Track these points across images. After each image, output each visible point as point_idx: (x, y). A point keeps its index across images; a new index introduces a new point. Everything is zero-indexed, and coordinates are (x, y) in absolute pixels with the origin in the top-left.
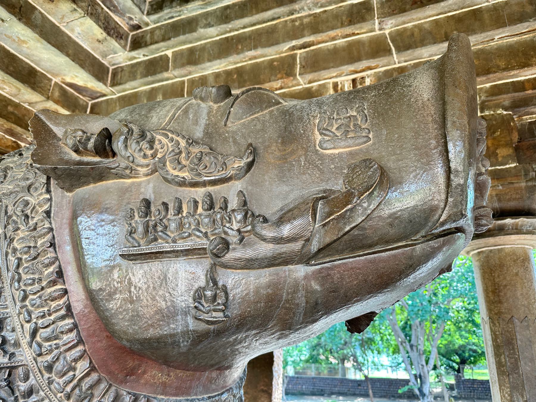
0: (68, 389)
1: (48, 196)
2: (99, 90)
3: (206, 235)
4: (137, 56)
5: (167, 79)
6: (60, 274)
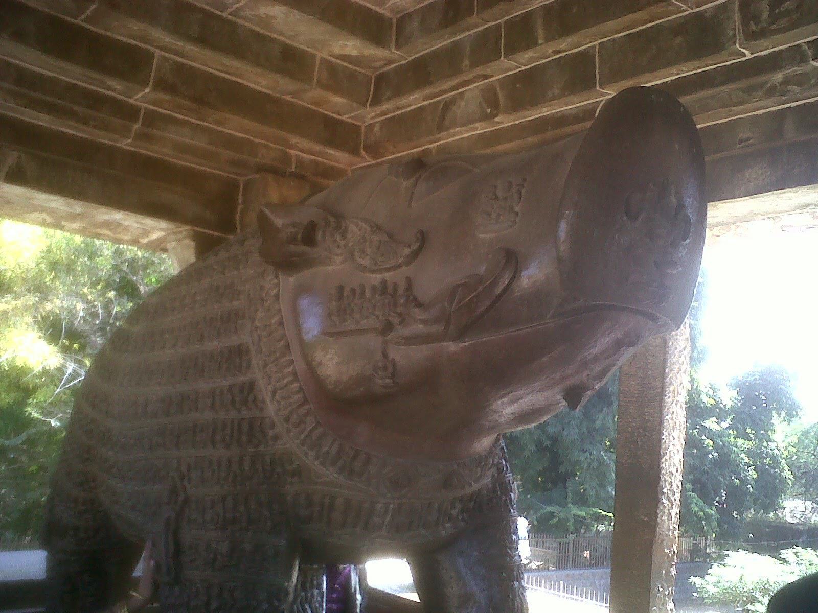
0: (302, 436)
1: (275, 281)
3: (377, 317)
6: (287, 347)
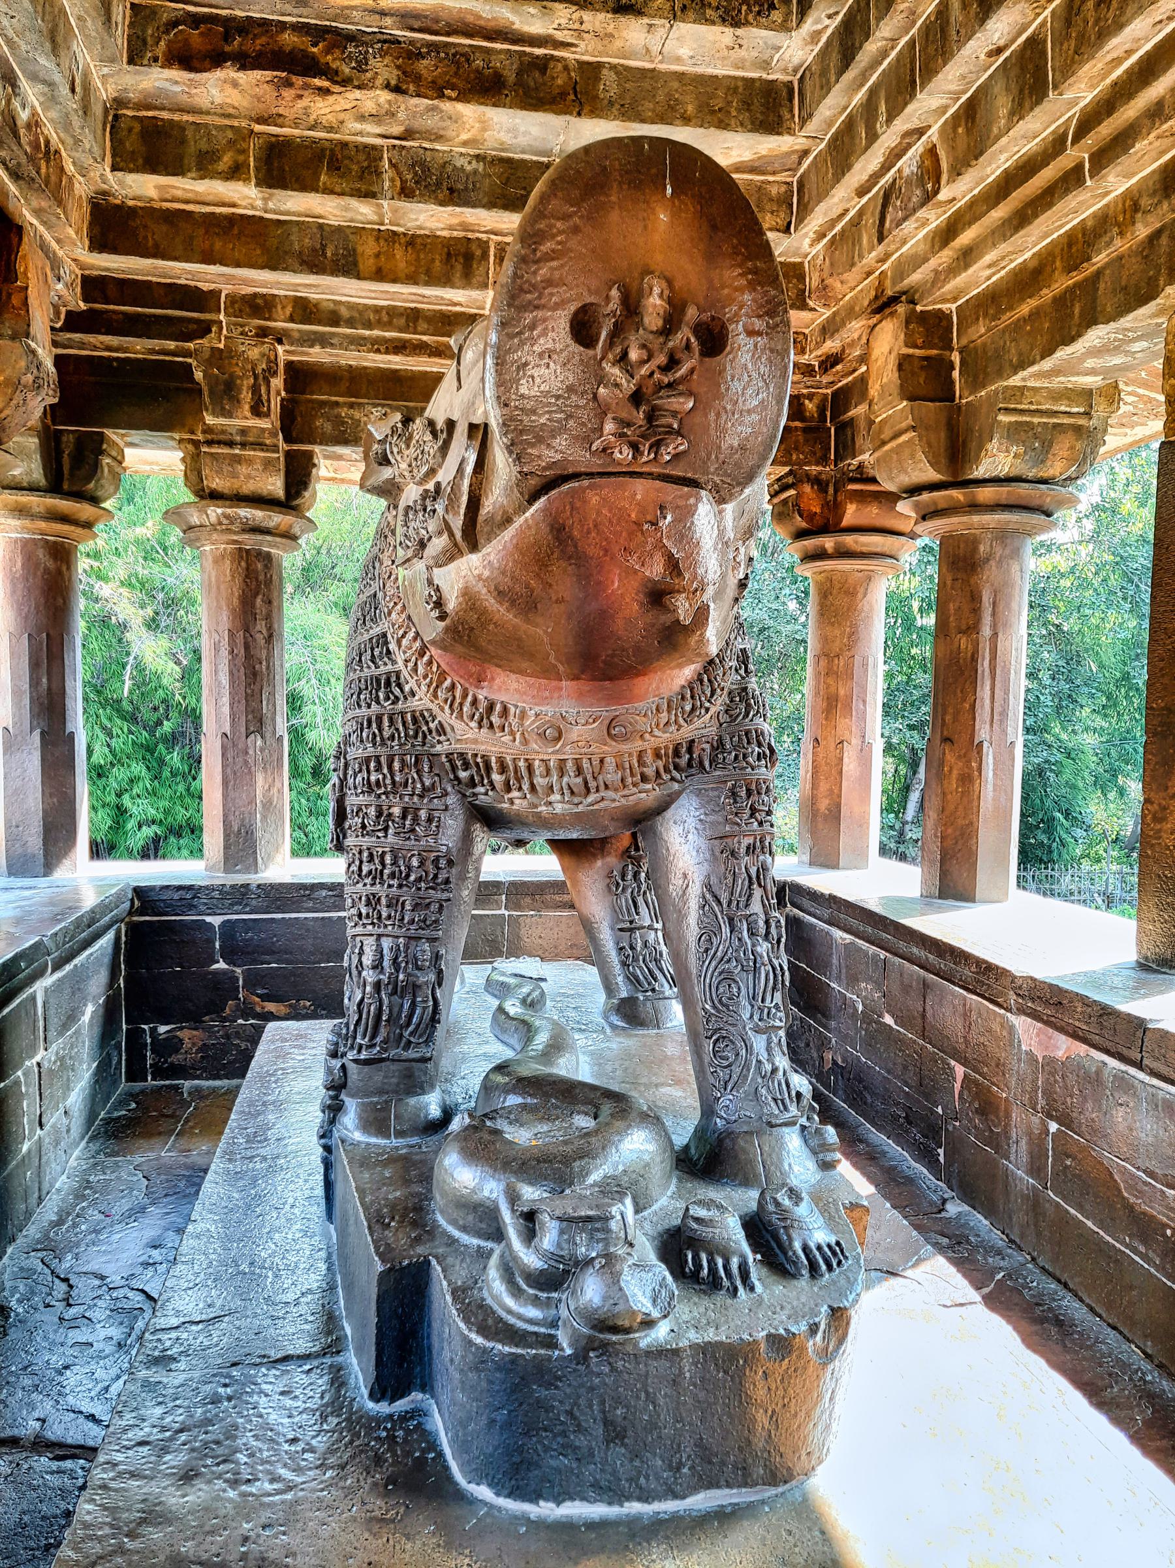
2: (785, 149)
4: (820, 27)
5: (884, 54)
